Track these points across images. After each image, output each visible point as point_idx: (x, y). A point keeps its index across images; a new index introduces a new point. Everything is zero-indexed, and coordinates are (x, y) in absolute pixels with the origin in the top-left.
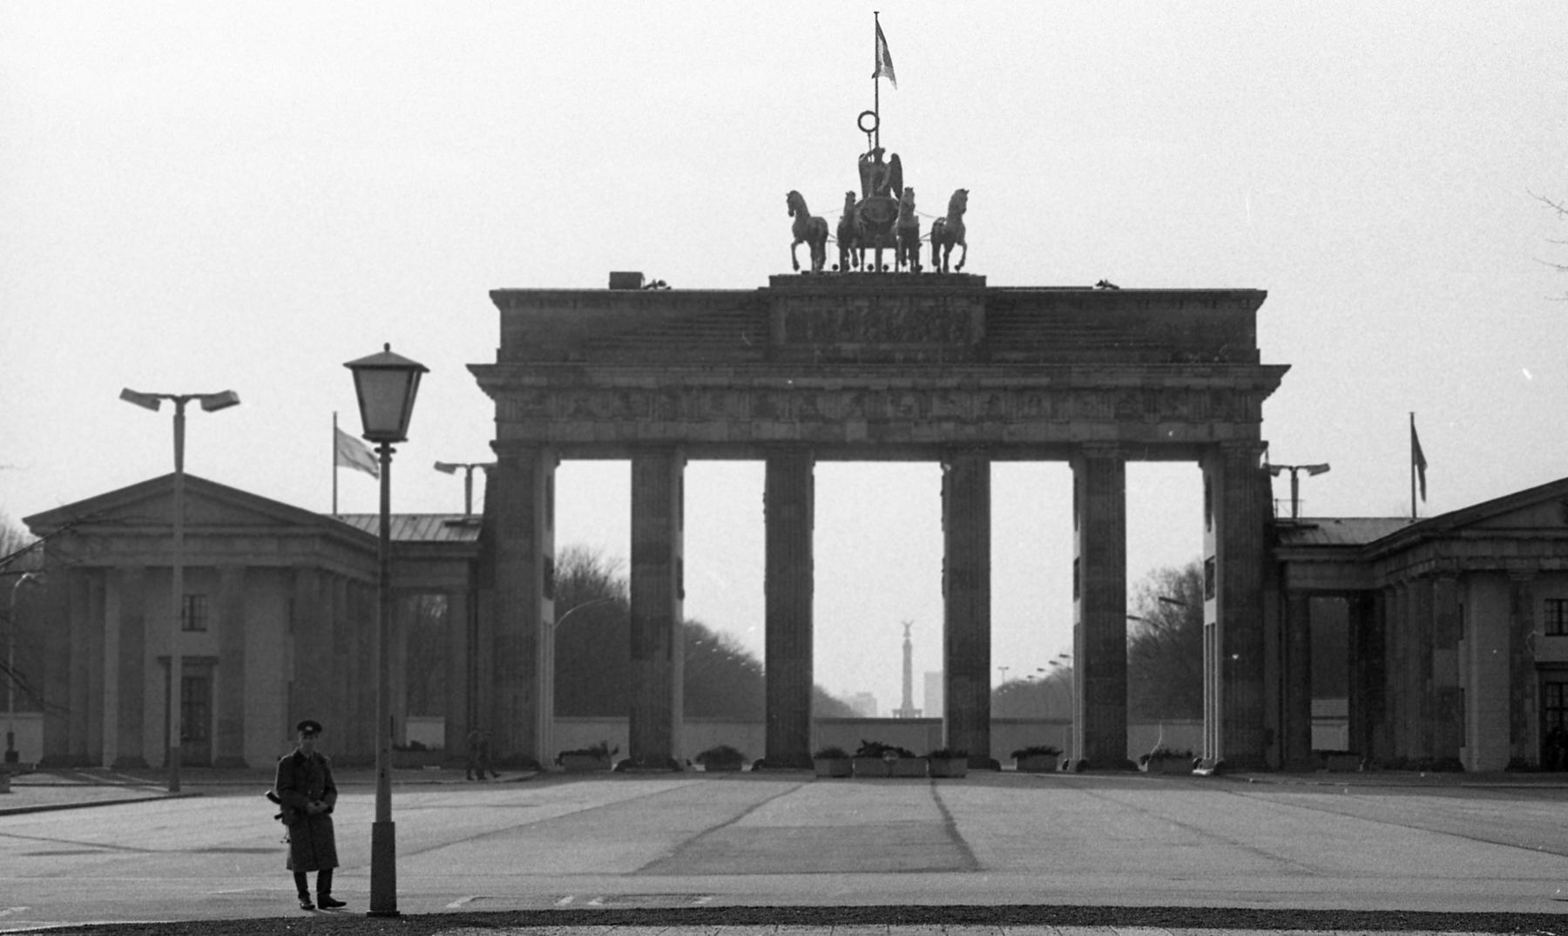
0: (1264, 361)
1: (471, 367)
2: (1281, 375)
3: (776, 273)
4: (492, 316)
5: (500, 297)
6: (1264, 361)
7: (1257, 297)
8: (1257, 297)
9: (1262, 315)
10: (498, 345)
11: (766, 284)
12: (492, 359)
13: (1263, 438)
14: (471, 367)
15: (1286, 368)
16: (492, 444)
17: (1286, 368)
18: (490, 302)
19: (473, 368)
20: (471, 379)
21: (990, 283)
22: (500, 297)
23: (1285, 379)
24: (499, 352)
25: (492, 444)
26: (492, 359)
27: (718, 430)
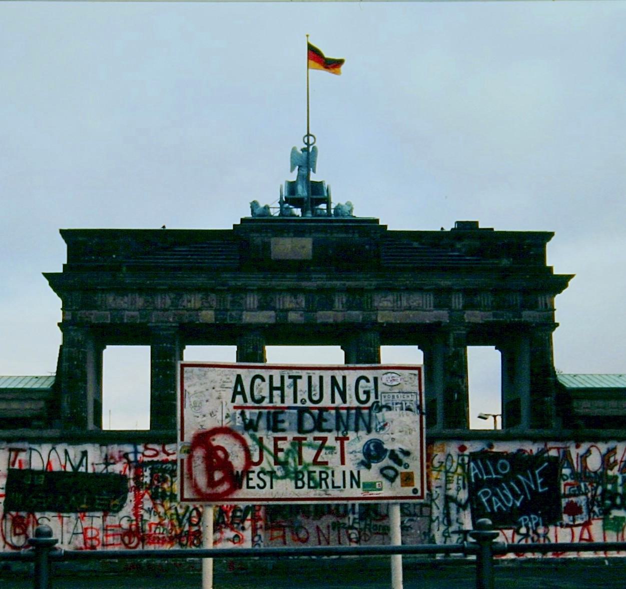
0: (556, 272)
1: (46, 275)
2: (569, 280)
3: (243, 217)
4: (63, 247)
5: (65, 234)
6: (556, 272)
7: (548, 236)
8: (548, 236)
9: (549, 245)
10: (65, 262)
11: (239, 223)
12: (60, 270)
13: (556, 321)
14: (46, 275)
15: (571, 276)
16: (59, 324)
17: (571, 276)
18: (60, 236)
19: (47, 275)
20: (47, 282)
21: (381, 223)
22: (65, 234)
23: (570, 283)
24: (64, 265)
25: (59, 324)
26: (61, 271)
27: (208, 316)
